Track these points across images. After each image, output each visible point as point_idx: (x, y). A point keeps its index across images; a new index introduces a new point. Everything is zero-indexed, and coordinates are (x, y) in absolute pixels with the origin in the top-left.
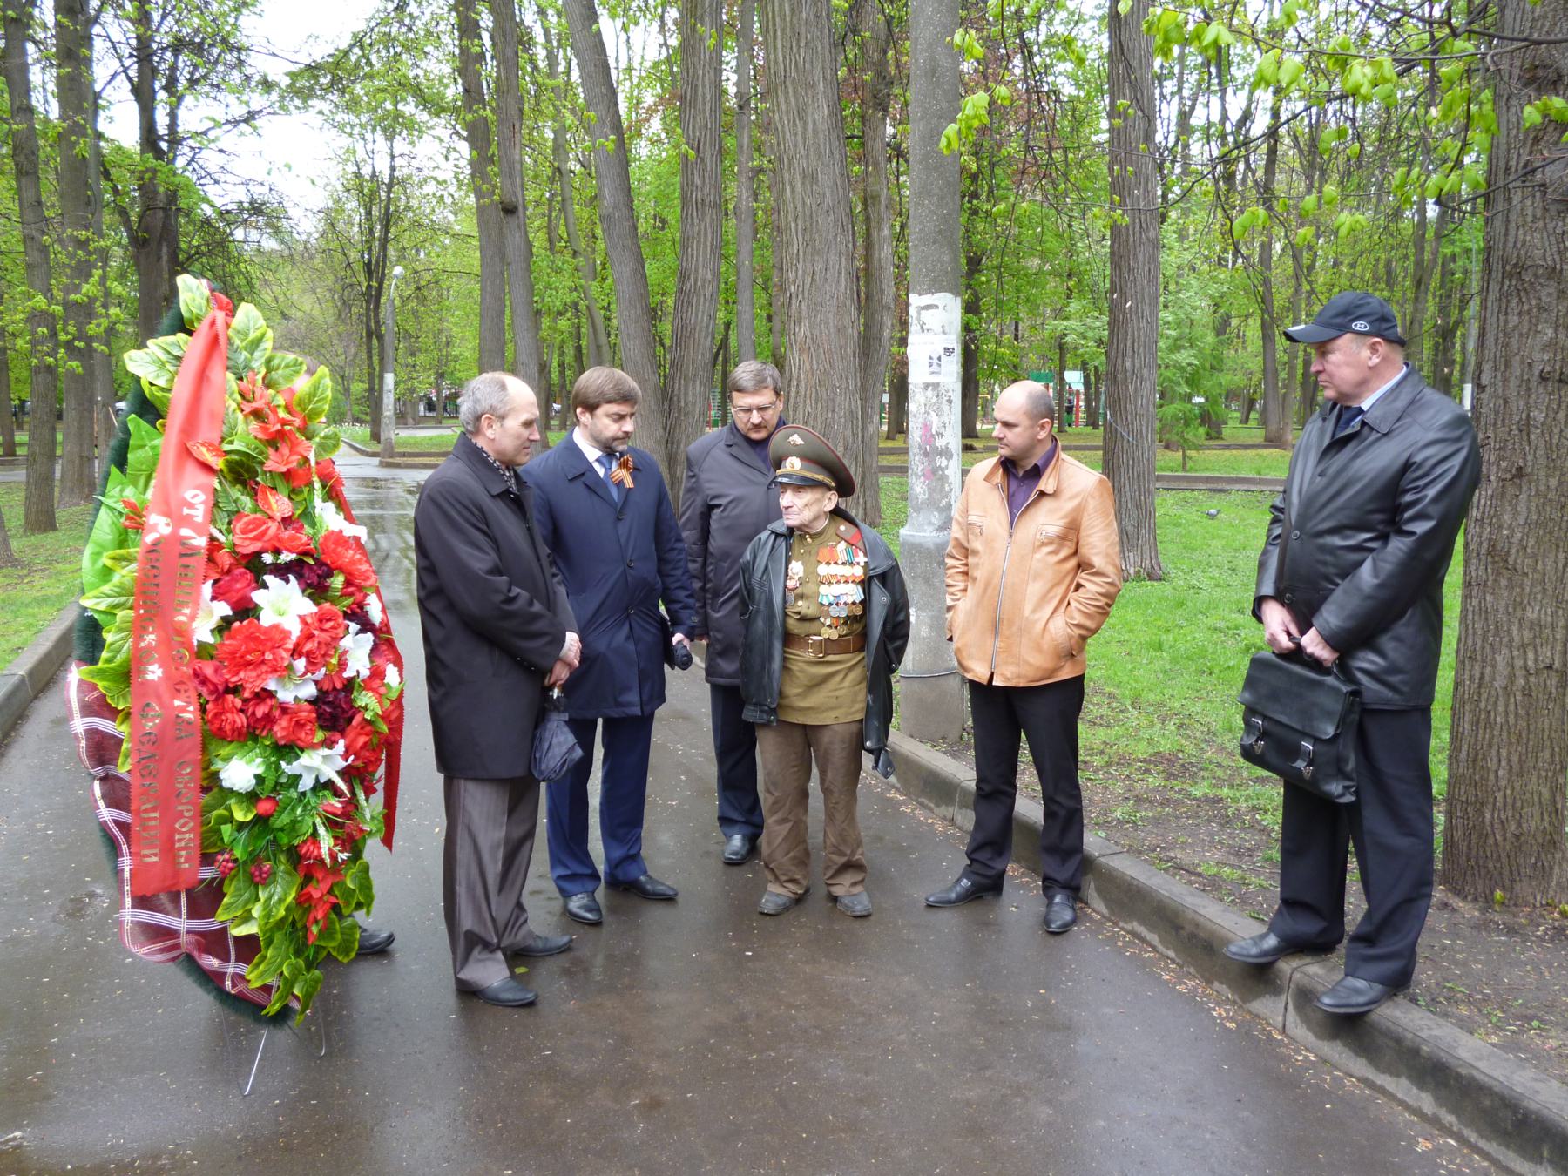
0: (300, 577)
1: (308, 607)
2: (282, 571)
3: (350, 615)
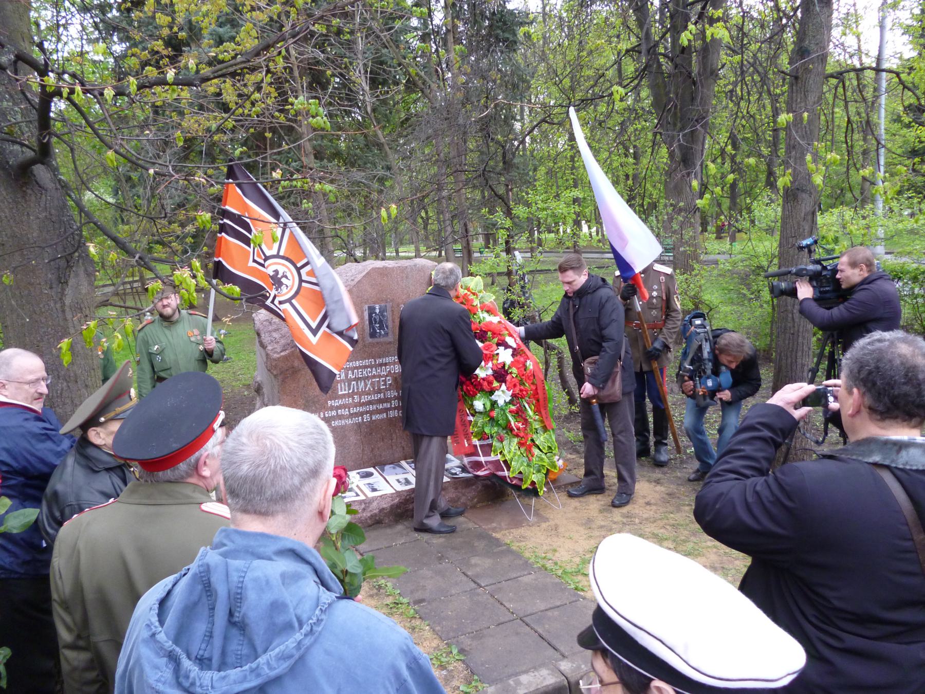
3: (498, 345)
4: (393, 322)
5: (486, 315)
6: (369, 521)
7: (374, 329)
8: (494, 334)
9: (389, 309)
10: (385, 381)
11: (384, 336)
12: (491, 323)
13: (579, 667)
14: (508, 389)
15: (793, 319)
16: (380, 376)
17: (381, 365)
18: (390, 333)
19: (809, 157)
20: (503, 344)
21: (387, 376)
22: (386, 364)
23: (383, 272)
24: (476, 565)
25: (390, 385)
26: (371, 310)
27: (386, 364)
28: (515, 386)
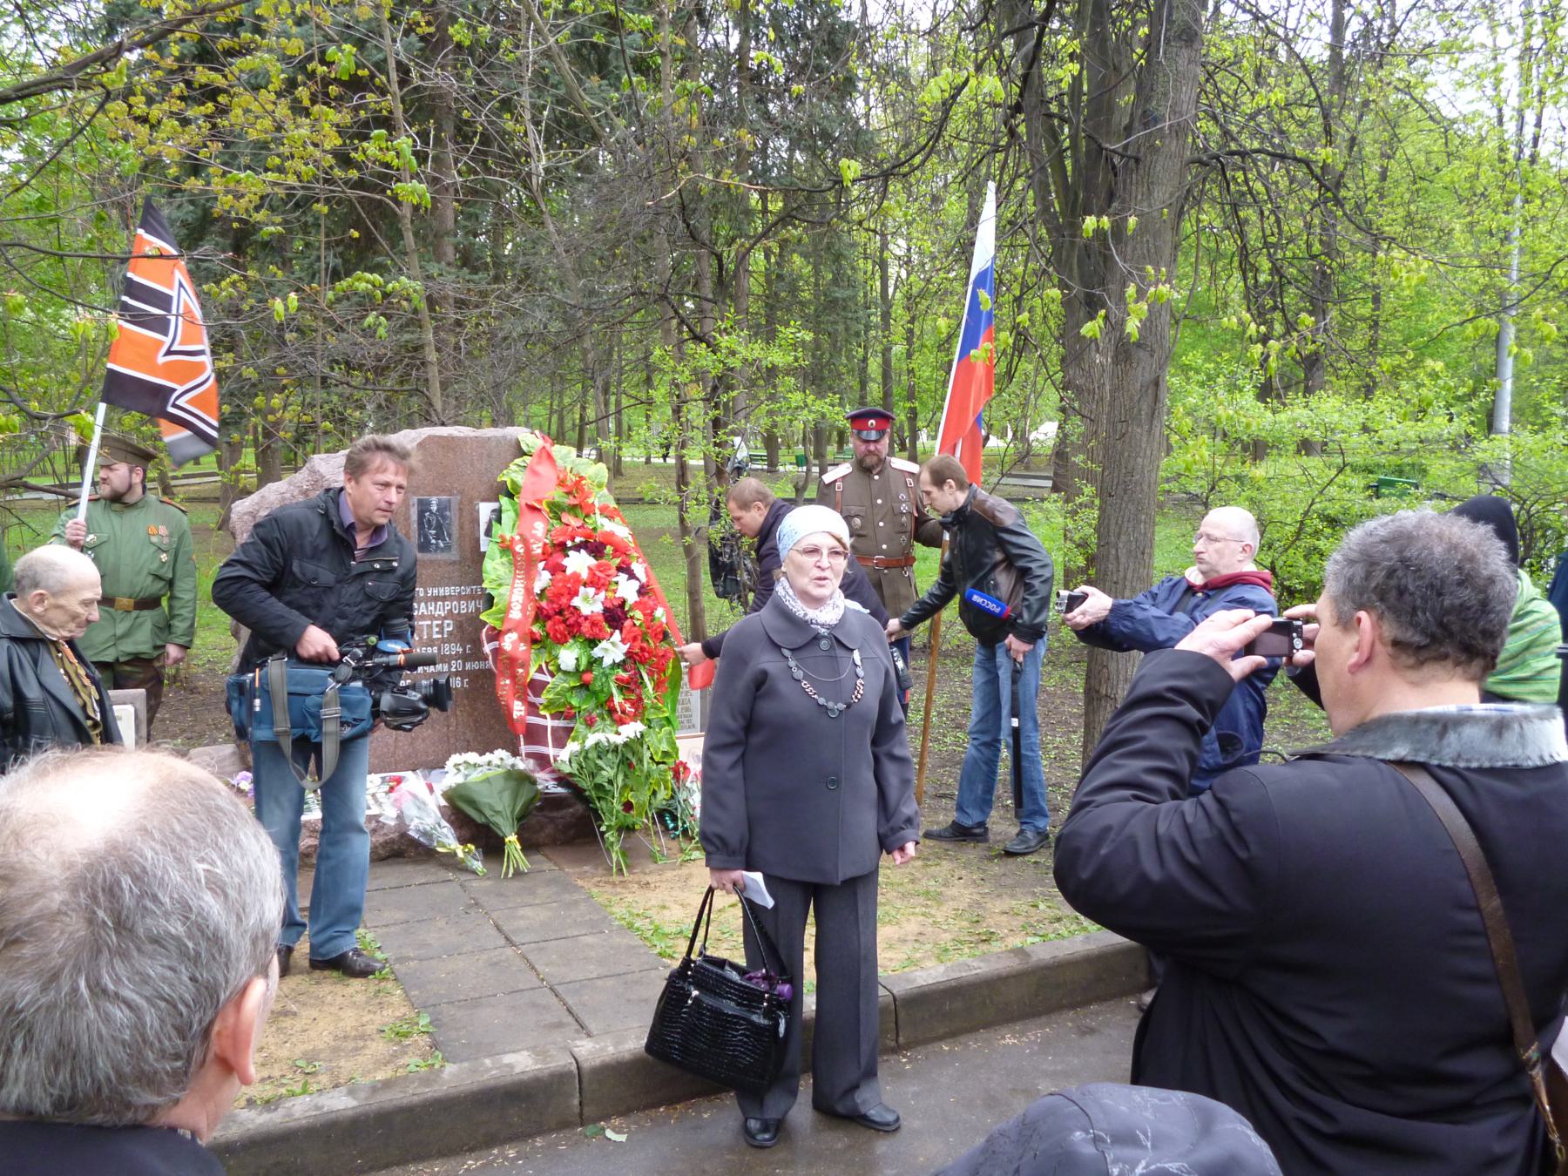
0: (586, 548)
1: (592, 561)
2: (577, 548)
3: (619, 569)
4: (461, 528)
5: (605, 521)
6: (381, 852)
7: (426, 537)
8: (616, 550)
9: (455, 506)
10: (441, 627)
11: (442, 550)
12: (612, 534)
13: (602, 1049)
14: (623, 641)
15: (1117, 558)
16: (432, 618)
17: (436, 599)
18: (455, 547)
19: (1131, 290)
20: (625, 569)
21: (445, 618)
22: (444, 599)
23: (449, 443)
24: (522, 917)
25: (450, 633)
26: (424, 506)
27: (444, 599)
28: (635, 639)
